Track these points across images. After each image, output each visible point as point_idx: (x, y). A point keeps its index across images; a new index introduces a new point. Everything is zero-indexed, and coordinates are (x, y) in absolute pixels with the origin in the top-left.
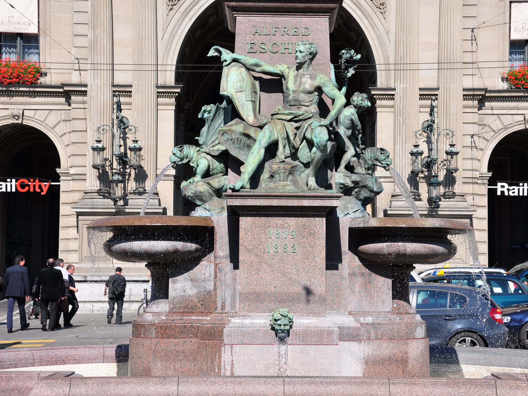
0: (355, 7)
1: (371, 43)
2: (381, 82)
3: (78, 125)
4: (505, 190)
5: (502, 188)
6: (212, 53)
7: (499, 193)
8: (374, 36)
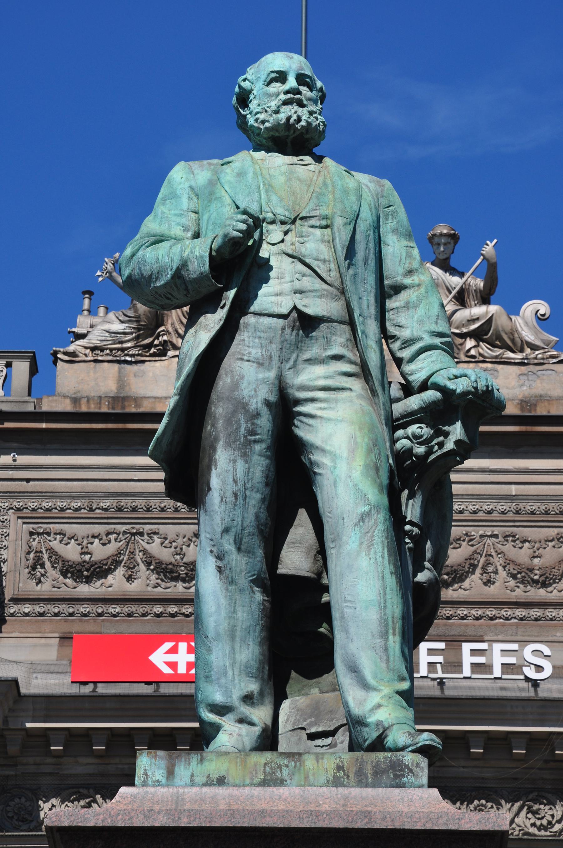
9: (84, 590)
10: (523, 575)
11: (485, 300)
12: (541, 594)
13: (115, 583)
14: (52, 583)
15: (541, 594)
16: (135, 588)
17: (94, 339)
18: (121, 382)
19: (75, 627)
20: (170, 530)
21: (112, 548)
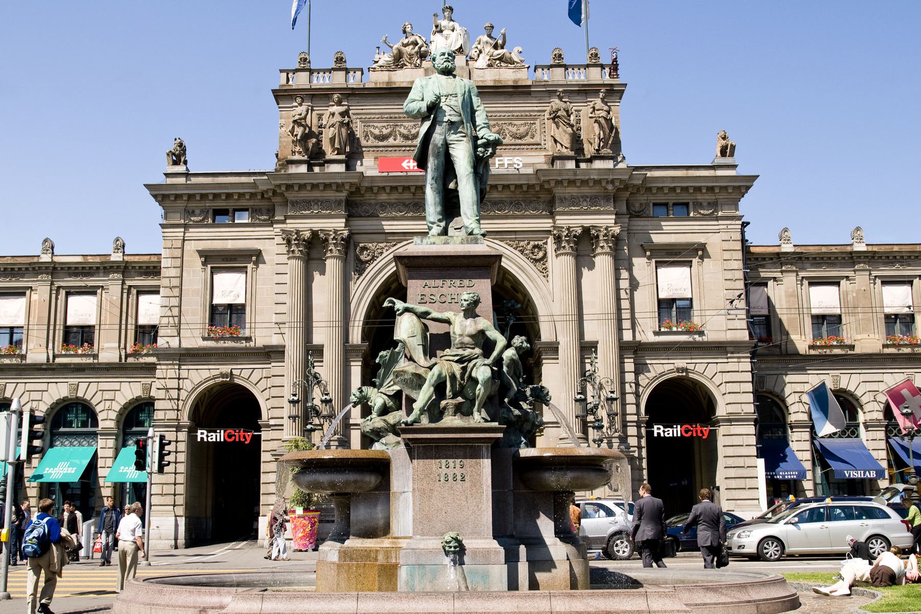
0: (520, 272)
1: (536, 302)
3: (277, 381)
4: (661, 431)
5: (658, 430)
6: (386, 304)
7: (656, 435)
8: (539, 296)
9: (381, 144)
11: (502, 48)
12: (519, 141)
13: (391, 141)
14: (372, 142)
15: (519, 141)
16: (397, 142)
17: (380, 63)
18: (390, 78)
19: (379, 155)
20: (406, 124)
21: (389, 130)
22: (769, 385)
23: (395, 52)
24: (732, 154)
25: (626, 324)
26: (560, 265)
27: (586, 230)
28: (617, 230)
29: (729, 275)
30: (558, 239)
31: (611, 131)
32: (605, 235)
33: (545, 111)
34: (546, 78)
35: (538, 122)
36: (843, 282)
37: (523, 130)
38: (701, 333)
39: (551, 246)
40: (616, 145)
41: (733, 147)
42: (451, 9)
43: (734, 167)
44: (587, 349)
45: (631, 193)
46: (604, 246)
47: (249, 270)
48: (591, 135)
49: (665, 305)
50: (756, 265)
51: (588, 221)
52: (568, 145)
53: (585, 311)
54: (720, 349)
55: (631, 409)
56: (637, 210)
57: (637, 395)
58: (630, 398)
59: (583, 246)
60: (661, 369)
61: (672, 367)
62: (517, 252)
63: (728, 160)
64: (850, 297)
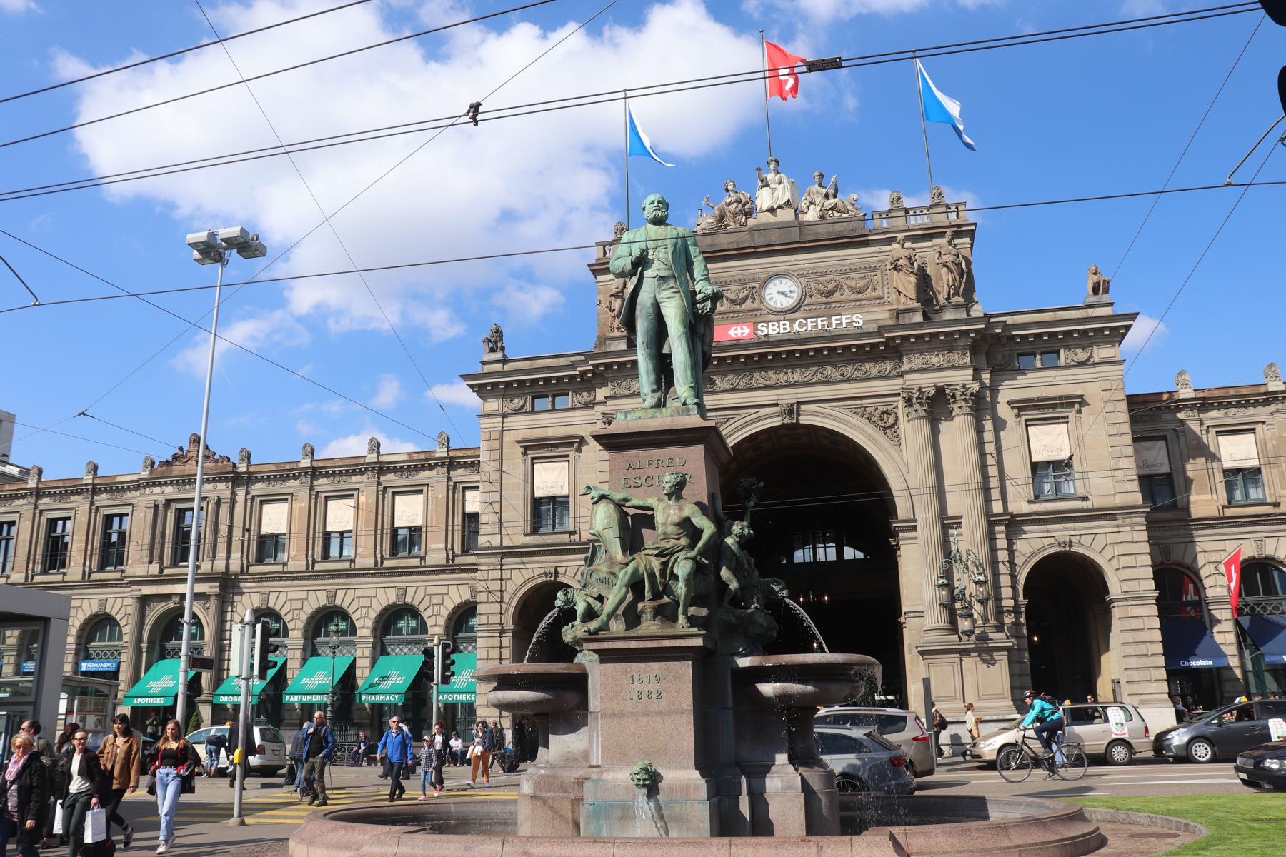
2: (901, 515)
10: (853, 289)
11: (835, 196)
12: (860, 296)
20: (733, 288)
22: (1176, 555)
23: (717, 213)
24: (1106, 291)
25: (995, 494)
26: (913, 429)
27: (940, 390)
28: (975, 387)
29: (1114, 430)
30: (909, 402)
31: (962, 277)
32: (963, 394)
33: (884, 261)
34: (885, 225)
35: (879, 273)
36: (1259, 428)
37: (862, 283)
38: (1084, 499)
39: (901, 411)
40: (970, 289)
41: (1107, 283)
42: (777, 162)
43: (1110, 305)
44: (947, 524)
45: (991, 345)
46: (960, 408)
47: (571, 459)
48: (943, 281)
49: (1037, 469)
50: (1150, 416)
51: (942, 378)
52: (914, 296)
53: (948, 481)
54: (1106, 514)
55: (1006, 592)
56: (1000, 362)
57: (1014, 577)
58: (1005, 580)
59: (937, 405)
60: (1034, 545)
61: (1052, 541)
62: (864, 420)
63: (1105, 298)
64: (1270, 447)
